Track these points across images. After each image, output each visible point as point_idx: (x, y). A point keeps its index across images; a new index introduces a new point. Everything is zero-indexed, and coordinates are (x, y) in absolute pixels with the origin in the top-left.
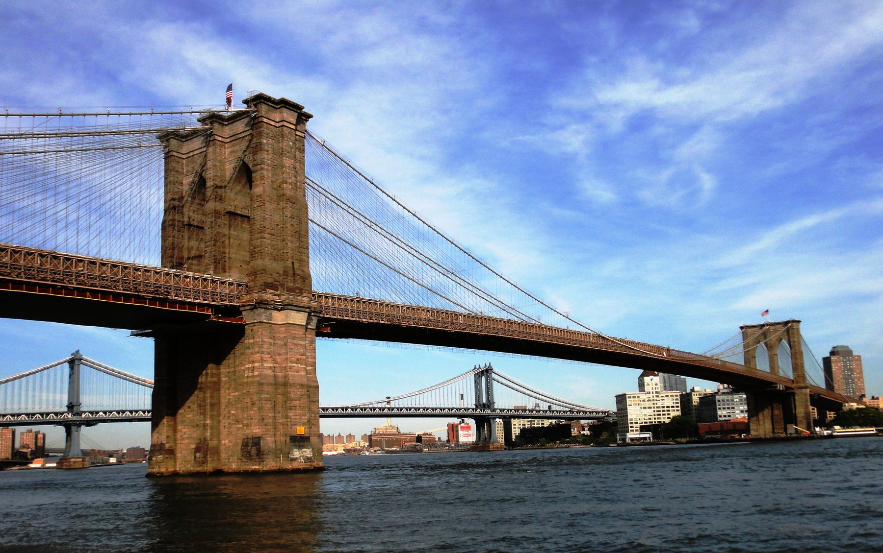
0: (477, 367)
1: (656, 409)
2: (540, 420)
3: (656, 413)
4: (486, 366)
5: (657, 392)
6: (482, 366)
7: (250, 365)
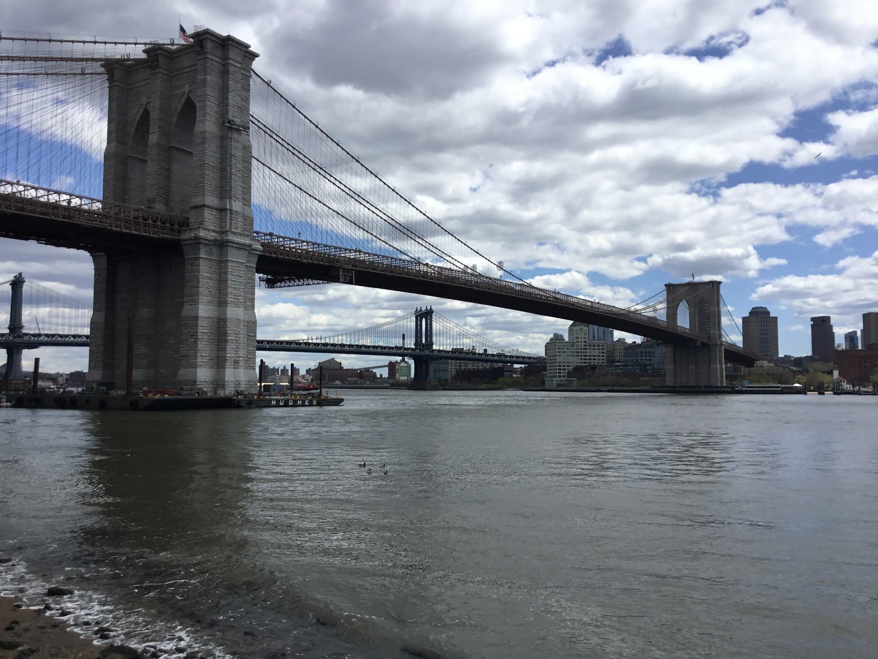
0: (419, 310)
1: (583, 358)
2: (476, 362)
3: (583, 361)
4: (427, 309)
5: (585, 342)
6: (424, 309)
7: (190, 298)
